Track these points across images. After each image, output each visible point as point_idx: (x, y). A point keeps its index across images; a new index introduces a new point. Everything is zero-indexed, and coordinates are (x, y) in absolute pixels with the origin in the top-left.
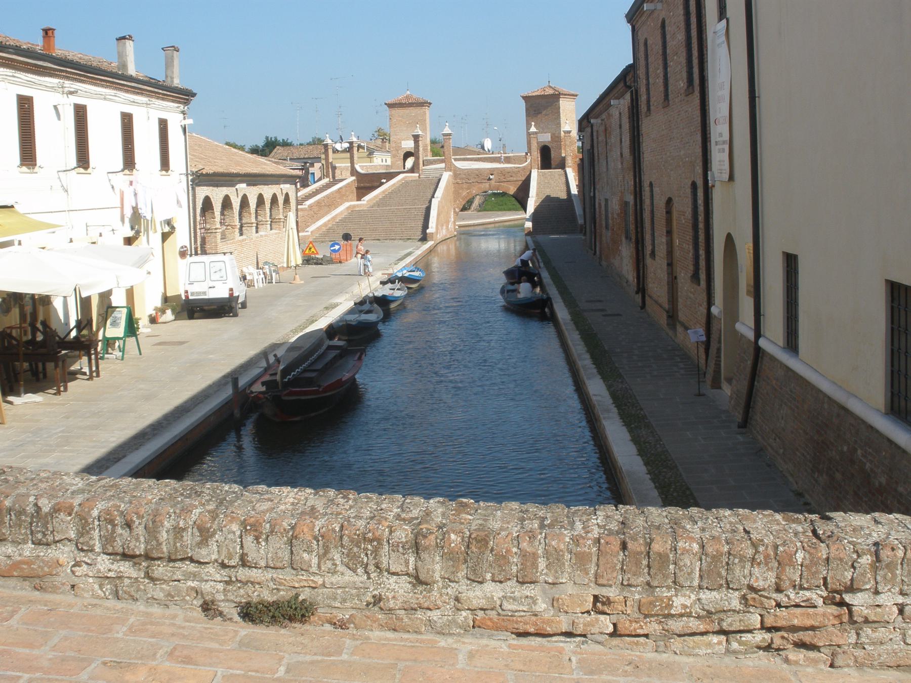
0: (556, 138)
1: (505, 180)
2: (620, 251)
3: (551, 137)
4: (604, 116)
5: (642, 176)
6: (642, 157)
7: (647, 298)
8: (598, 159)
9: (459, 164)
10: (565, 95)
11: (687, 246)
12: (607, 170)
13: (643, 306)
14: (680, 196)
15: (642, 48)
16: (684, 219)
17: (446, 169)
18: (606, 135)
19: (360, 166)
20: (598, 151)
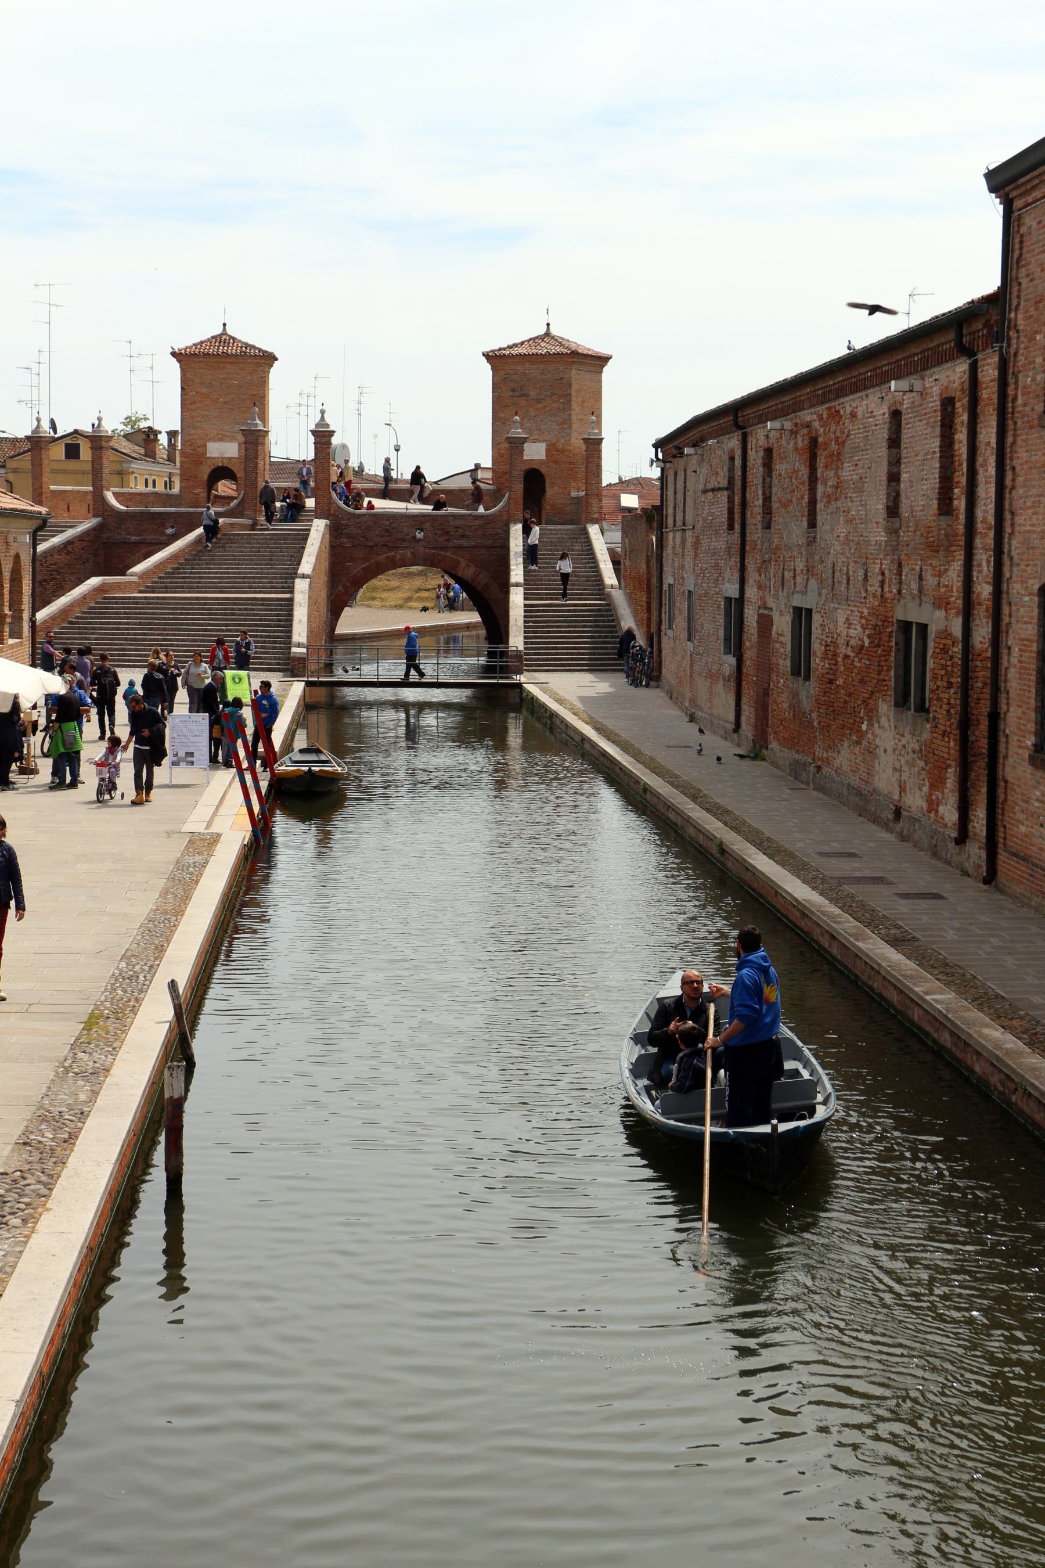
2: (861, 735)
3: (547, 451)
5: (1006, 570)
6: (1007, 524)
7: (1002, 857)
12: (811, 542)
13: (990, 877)
18: (813, 458)
19: (114, 493)
20: (767, 499)
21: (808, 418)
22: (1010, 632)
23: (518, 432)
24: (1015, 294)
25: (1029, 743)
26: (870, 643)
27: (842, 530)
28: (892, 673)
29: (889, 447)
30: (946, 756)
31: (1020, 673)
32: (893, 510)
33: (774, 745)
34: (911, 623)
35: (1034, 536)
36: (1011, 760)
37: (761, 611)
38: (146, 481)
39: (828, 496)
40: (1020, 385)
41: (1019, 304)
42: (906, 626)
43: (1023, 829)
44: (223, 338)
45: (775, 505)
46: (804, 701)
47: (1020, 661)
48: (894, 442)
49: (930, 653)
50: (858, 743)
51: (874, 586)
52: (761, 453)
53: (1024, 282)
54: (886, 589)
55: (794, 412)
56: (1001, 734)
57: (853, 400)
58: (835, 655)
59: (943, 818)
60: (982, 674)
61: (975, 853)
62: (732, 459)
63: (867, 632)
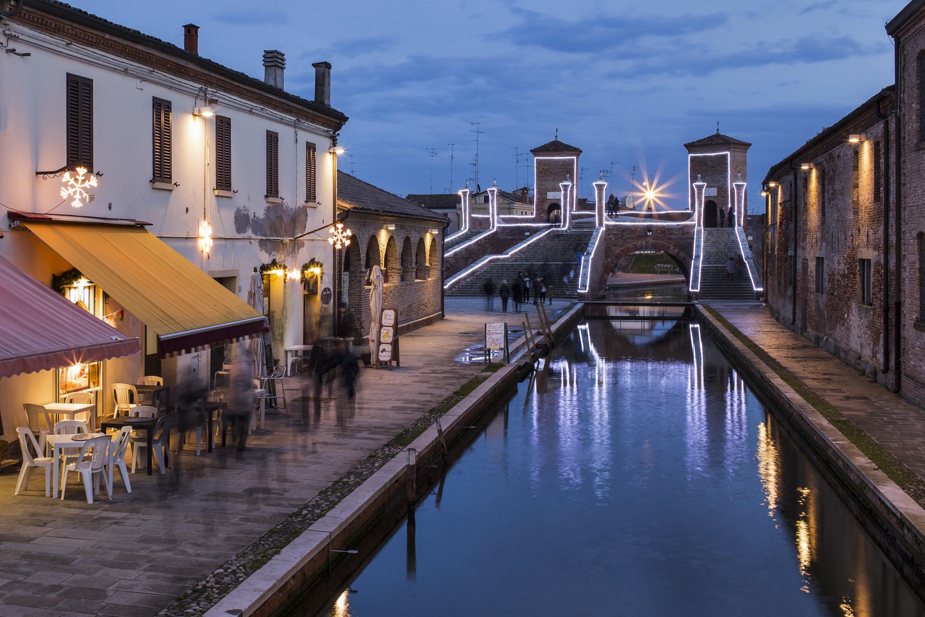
7: (903, 378)
21: (821, 160)
24: (902, 85)
27: (835, 216)
30: (879, 327)
31: (910, 281)
33: (809, 330)
34: (864, 260)
35: (914, 208)
36: (907, 327)
38: (522, 212)
39: (830, 199)
40: (907, 130)
41: (904, 90)
42: (862, 261)
43: (912, 363)
46: (821, 305)
47: (910, 274)
52: (803, 181)
53: (907, 78)
55: (815, 158)
59: (878, 360)
61: (891, 378)
62: (791, 185)
63: (847, 266)
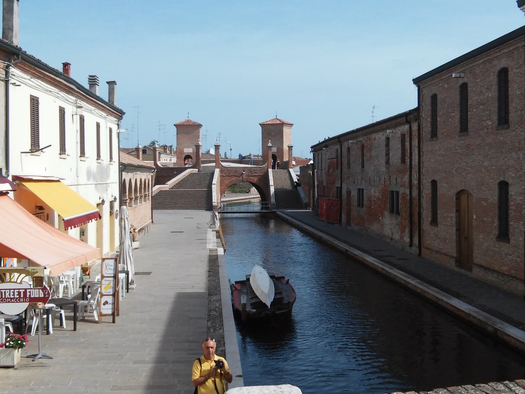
0: (280, 150)
1: (252, 175)
4: (360, 139)
6: (421, 165)
7: (423, 249)
8: (349, 164)
9: (224, 164)
10: (287, 124)
11: (490, 220)
13: (420, 254)
14: (481, 190)
15: (428, 101)
16: (485, 203)
17: (216, 167)
22: (423, 192)
23: (270, 144)
25: (429, 220)
26: (381, 197)
28: (388, 204)
29: (386, 147)
32: (387, 162)
34: (394, 191)
37: (347, 190)
42: (392, 192)
43: (428, 242)
44: (188, 121)
45: (351, 162)
48: (387, 145)
49: (400, 198)
50: (379, 223)
51: (382, 182)
53: (424, 106)
54: (386, 183)
56: (421, 218)
57: (374, 135)
58: (371, 201)
60: (416, 202)
62: (337, 151)
